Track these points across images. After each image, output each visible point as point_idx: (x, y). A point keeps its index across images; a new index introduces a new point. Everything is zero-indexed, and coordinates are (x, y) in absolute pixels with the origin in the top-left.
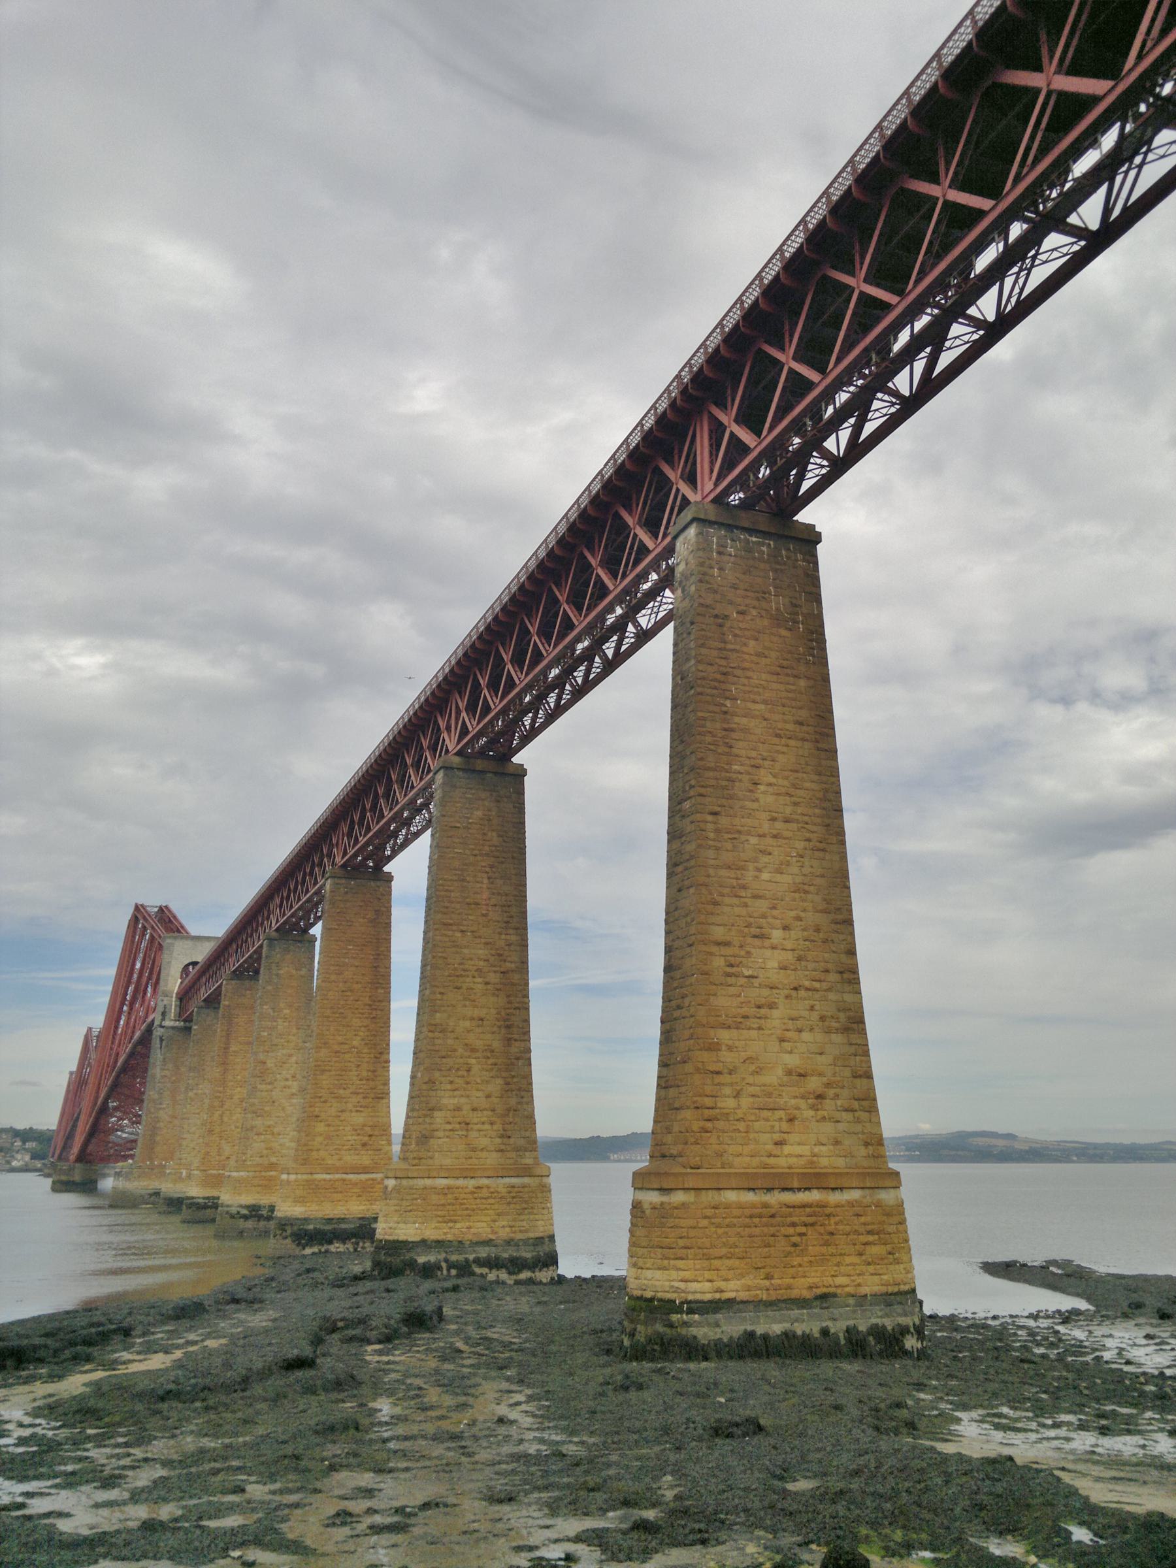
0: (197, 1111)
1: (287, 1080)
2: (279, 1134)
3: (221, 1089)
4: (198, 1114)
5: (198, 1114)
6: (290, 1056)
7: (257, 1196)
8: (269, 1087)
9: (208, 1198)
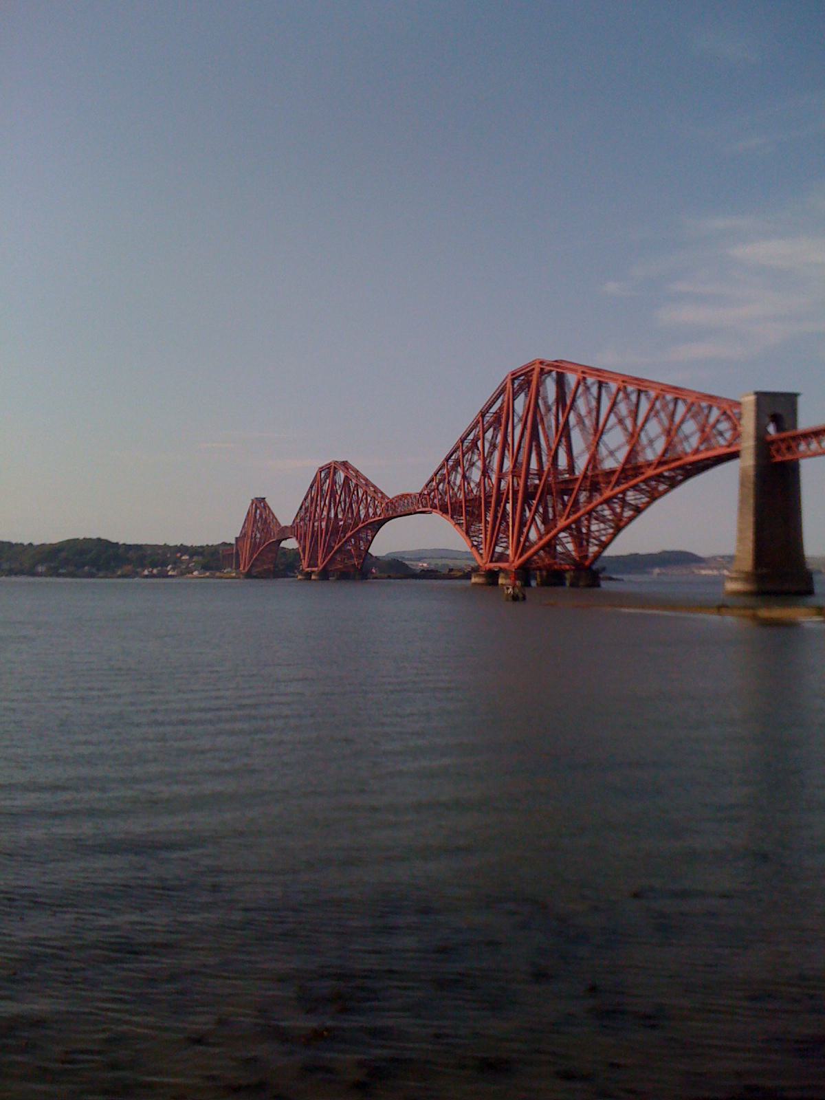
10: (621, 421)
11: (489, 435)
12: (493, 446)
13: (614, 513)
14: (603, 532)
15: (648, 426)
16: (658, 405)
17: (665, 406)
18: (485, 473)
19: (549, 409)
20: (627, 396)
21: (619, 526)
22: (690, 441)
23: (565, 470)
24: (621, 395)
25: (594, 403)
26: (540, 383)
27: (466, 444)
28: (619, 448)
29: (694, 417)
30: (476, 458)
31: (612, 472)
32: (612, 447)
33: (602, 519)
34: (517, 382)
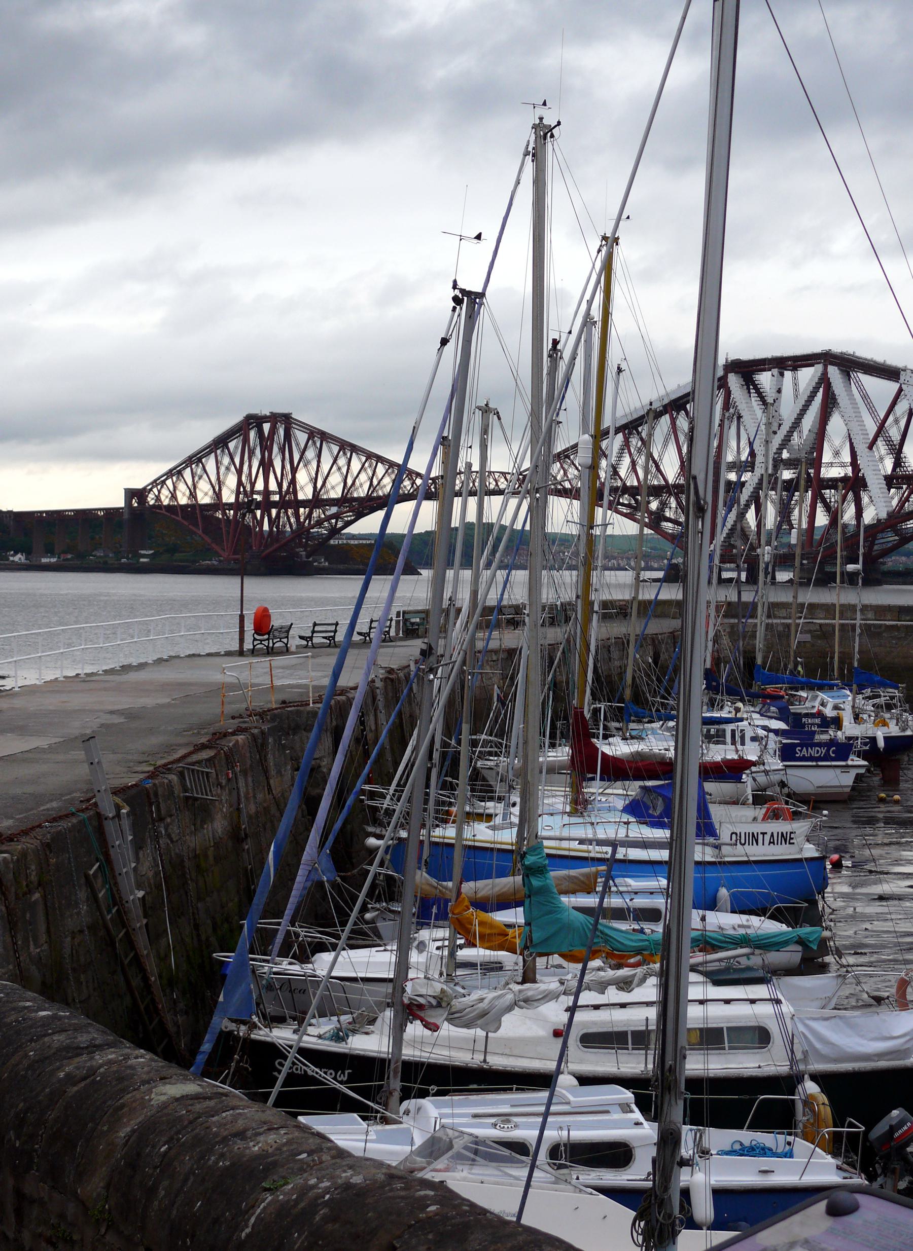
10: (339, 469)
16: (367, 465)
17: (370, 466)
20: (345, 454)
24: (341, 453)
26: (273, 431)
32: (333, 484)
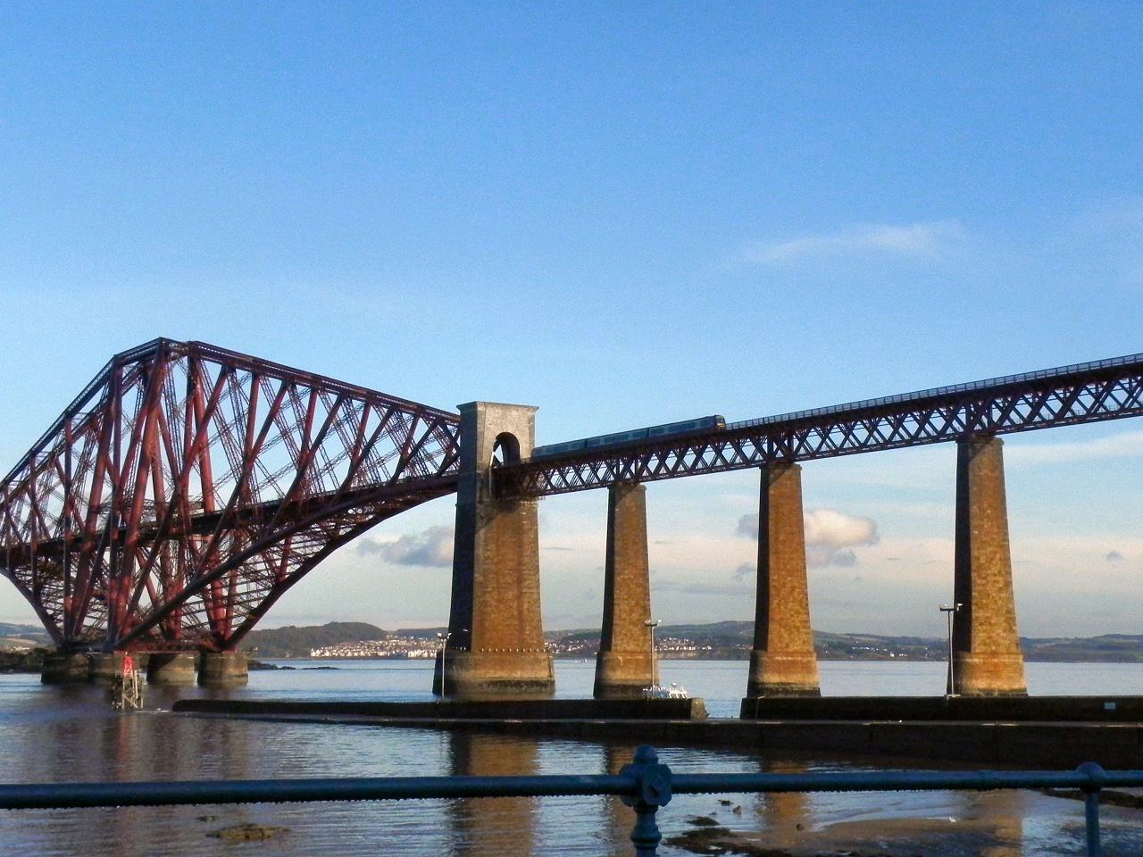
0: (626, 597)
1: (995, 575)
2: (995, 625)
3: (776, 578)
4: (627, 599)
5: (627, 599)
6: (995, 553)
7: (988, 681)
8: (984, 581)
9: (778, 684)
10: (285, 434)
11: (79, 446)
12: (84, 465)
13: (272, 569)
14: (255, 595)
15: (325, 442)
16: (341, 413)
18: (70, 503)
19: (174, 412)
20: (296, 399)
21: (281, 584)
22: (386, 464)
23: (198, 502)
24: (287, 396)
25: (246, 406)
27: (40, 458)
28: (282, 472)
29: (390, 432)
30: (55, 480)
31: (270, 508)
32: (272, 471)
33: (254, 576)
34: (126, 370)
